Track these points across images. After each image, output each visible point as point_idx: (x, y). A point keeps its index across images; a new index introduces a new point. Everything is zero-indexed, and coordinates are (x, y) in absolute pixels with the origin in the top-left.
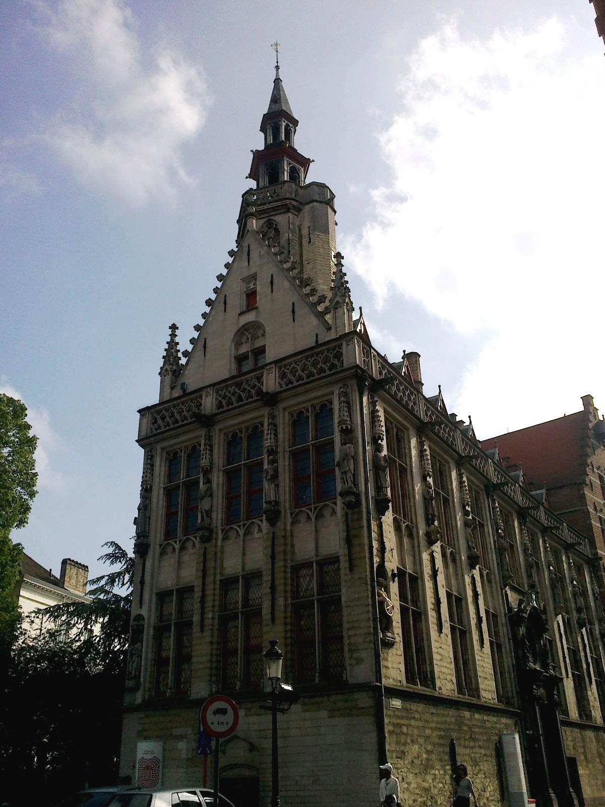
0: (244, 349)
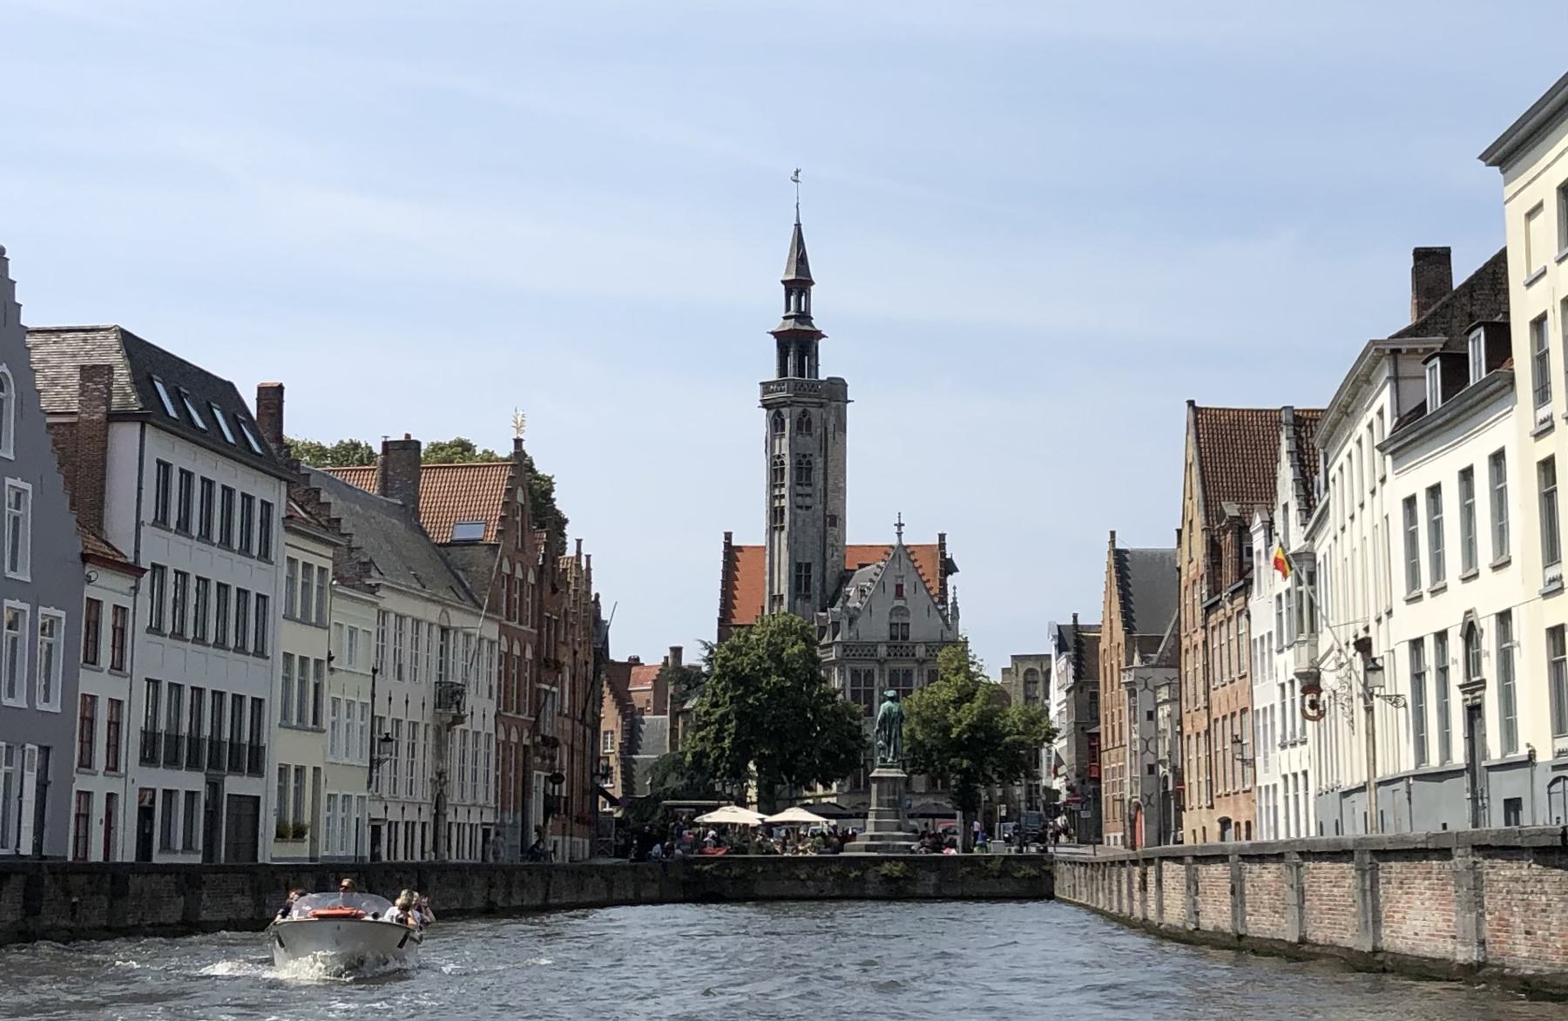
0: (895, 620)
